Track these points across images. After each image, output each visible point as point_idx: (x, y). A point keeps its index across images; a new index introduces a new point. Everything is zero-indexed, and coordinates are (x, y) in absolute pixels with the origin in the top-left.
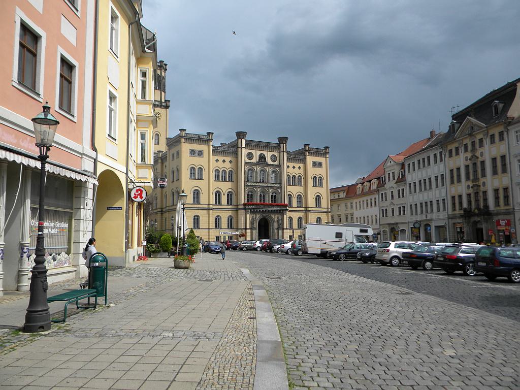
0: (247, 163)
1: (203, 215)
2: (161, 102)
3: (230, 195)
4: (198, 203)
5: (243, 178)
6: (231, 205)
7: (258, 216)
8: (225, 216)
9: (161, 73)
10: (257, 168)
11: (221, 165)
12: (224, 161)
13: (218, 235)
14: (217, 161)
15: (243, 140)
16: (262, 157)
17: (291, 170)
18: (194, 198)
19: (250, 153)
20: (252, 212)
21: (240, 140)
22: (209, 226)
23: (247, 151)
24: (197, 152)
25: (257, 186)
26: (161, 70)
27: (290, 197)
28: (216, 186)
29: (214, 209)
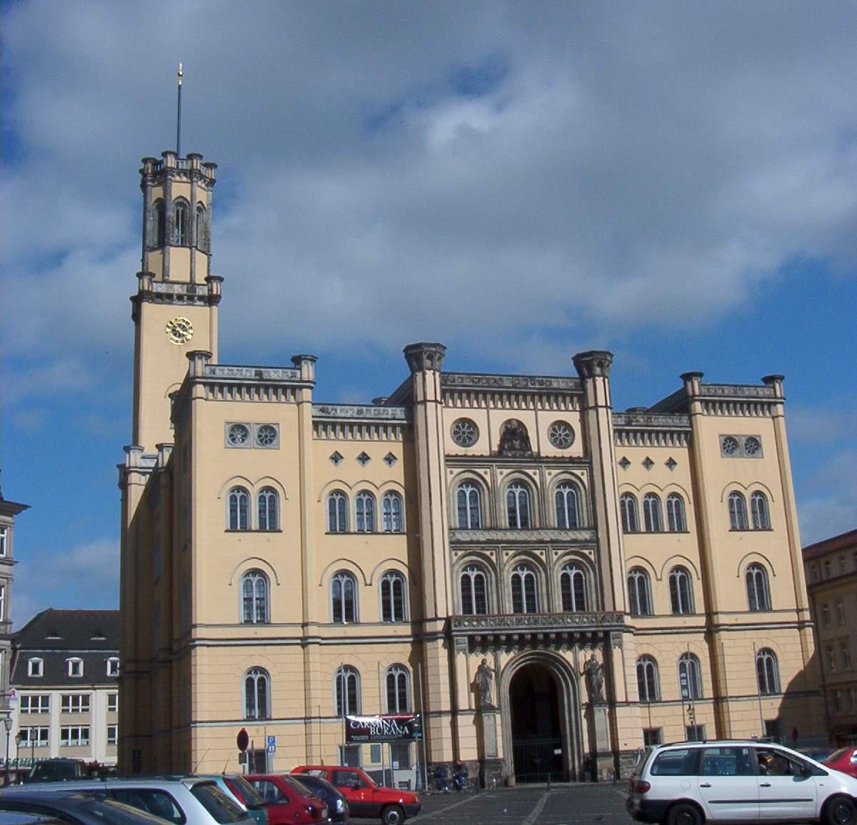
0: (452, 460)
1: (283, 666)
2: (192, 285)
3: (391, 590)
4: (264, 621)
5: (440, 515)
7: (505, 658)
10: (493, 476)
14: (336, 458)
15: (429, 374)
16: (514, 435)
17: (637, 480)
19: (464, 421)
21: (419, 375)
23: (451, 415)
24: (254, 432)
25: (498, 542)
27: (639, 581)
29: (325, 641)
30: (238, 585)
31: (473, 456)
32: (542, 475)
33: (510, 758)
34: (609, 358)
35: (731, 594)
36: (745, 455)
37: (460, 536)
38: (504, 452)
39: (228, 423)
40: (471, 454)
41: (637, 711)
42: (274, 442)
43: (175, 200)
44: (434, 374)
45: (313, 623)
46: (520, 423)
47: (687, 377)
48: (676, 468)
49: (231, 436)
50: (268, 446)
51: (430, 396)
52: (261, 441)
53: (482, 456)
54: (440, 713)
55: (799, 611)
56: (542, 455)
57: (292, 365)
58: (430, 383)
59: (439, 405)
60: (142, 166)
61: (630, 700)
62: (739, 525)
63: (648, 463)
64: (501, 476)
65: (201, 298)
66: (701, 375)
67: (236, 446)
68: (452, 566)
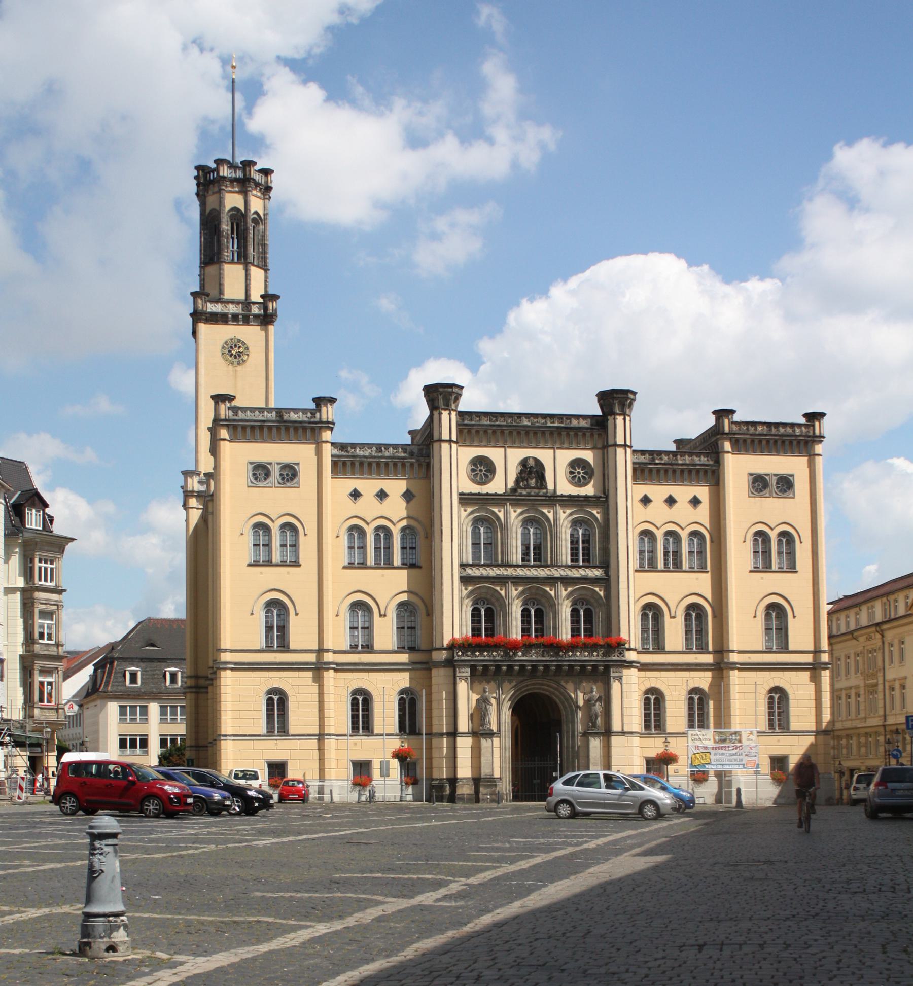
0: (465, 499)
2: (247, 303)
6: (412, 649)
8: (387, 691)
9: (246, 203)
11: (370, 510)
12: (382, 495)
13: (361, 756)
15: (445, 414)
16: (532, 472)
17: (659, 516)
18: (269, 628)
20: (479, 674)
21: (436, 413)
22: (321, 725)
24: (276, 472)
26: (244, 192)
28: (343, 585)
29: (340, 668)
30: (261, 614)
31: (487, 494)
32: (555, 514)
33: (508, 777)
34: (631, 396)
35: (745, 632)
36: (774, 495)
37: (470, 571)
38: (519, 491)
39: (251, 463)
40: (484, 492)
41: (636, 740)
42: (295, 480)
43: (229, 211)
44: (450, 414)
45: (328, 651)
46: (537, 461)
47: (721, 414)
48: (701, 507)
49: (254, 474)
50: (288, 484)
51: (445, 436)
52: (283, 479)
53: (496, 494)
54: (441, 735)
55: (817, 652)
56: (559, 493)
57: (313, 406)
58: (448, 423)
59: (454, 445)
60: (195, 173)
61: (626, 730)
62: (763, 563)
63: (671, 501)
64: (513, 516)
65: (256, 316)
66: (732, 412)
67: (260, 484)
68: (461, 600)
